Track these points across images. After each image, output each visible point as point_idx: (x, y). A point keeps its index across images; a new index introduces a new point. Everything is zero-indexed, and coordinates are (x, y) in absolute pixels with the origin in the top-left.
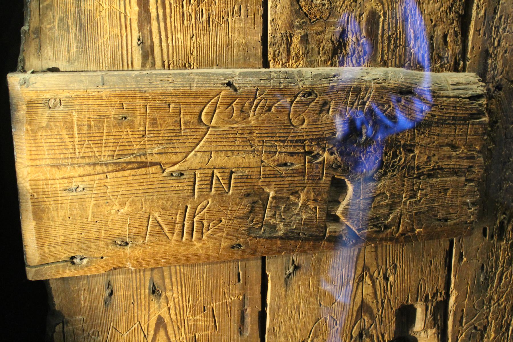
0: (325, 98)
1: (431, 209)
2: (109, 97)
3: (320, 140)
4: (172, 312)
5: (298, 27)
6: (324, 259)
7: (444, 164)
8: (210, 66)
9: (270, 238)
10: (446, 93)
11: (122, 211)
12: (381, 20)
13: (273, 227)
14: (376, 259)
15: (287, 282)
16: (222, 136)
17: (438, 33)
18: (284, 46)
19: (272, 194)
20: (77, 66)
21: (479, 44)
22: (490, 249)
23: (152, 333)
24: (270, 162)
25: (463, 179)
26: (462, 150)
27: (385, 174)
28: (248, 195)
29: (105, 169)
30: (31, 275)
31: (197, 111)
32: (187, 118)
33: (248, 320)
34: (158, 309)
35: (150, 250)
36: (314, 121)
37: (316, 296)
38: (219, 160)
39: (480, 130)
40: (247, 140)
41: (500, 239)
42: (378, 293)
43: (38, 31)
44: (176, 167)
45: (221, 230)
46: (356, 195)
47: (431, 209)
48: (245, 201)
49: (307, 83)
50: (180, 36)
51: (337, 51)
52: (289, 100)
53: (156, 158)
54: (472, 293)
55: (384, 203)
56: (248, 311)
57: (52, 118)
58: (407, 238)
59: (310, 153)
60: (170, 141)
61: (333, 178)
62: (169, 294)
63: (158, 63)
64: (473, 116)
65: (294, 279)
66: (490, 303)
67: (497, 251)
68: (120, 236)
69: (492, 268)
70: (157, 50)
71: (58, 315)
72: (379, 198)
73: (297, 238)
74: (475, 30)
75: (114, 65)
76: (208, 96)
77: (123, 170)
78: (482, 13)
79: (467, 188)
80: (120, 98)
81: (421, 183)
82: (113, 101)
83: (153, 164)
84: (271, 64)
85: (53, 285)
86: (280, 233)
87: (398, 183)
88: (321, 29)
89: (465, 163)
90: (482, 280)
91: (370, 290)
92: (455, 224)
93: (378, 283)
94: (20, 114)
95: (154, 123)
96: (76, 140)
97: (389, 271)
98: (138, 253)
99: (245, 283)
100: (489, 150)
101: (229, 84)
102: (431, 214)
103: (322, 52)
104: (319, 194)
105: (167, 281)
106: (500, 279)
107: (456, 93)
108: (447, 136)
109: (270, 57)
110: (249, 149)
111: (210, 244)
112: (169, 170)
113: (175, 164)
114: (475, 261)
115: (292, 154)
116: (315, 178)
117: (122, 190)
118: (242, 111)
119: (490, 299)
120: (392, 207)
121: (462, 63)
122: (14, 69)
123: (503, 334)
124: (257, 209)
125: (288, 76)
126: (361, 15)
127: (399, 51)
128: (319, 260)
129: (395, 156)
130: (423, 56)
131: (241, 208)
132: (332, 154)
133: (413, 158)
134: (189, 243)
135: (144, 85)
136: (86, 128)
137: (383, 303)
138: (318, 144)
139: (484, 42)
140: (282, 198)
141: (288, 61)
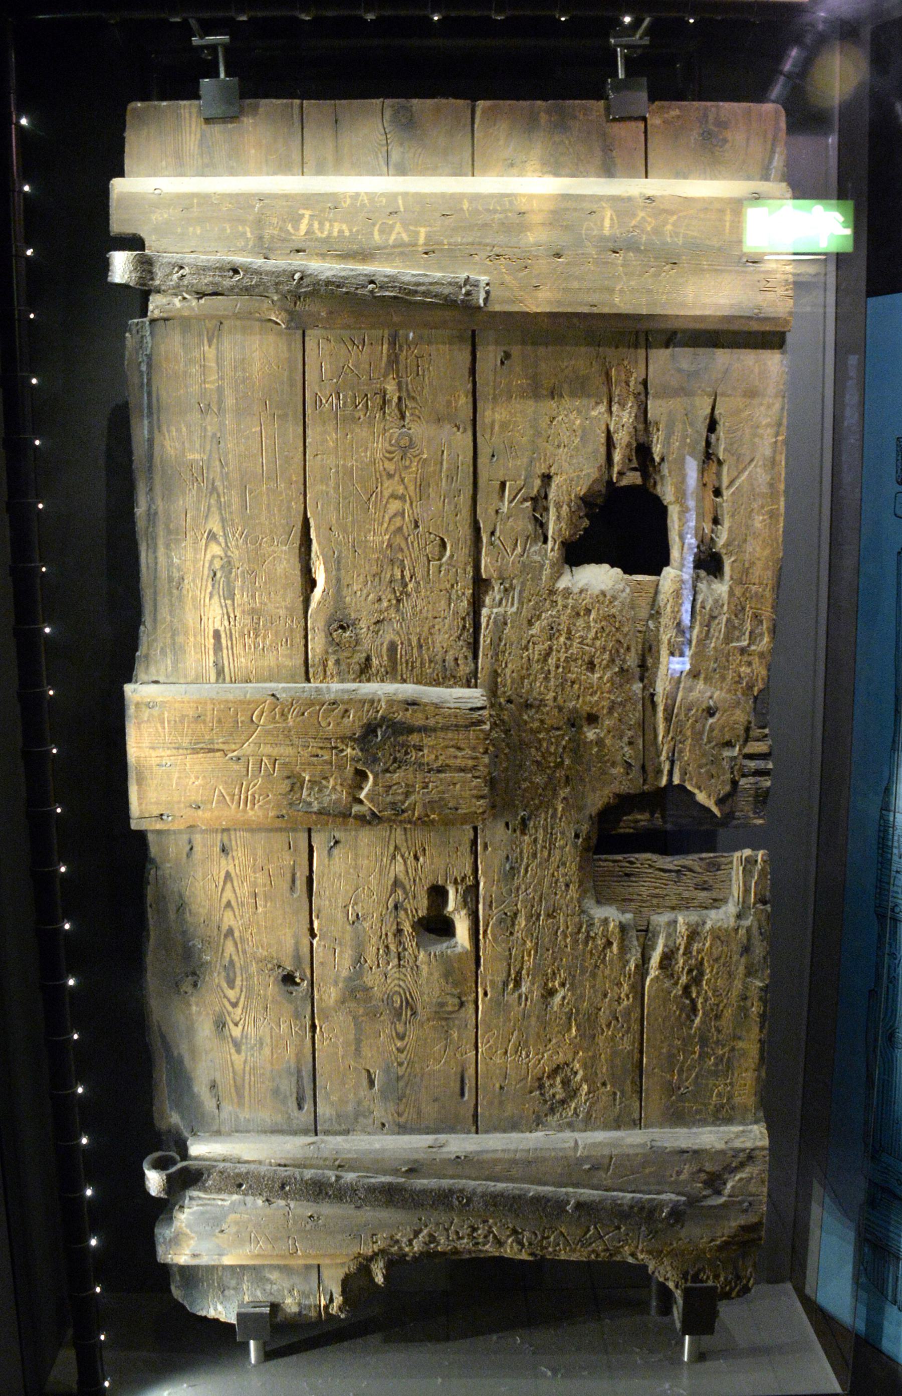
0: (346, 707)
1: (441, 799)
2: (189, 702)
3: (343, 739)
4: (237, 868)
5: (335, 652)
6: (360, 837)
7: (451, 762)
8: (265, 681)
9: (306, 812)
10: (448, 705)
11: (196, 783)
12: (399, 647)
13: (310, 804)
14: (406, 841)
15: (330, 854)
16: (268, 732)
17: (450, 657)
18: (321, 669)
19: (307, 778)
20: (171, 680)
21: (488, 666)
22: (513, 842)
23: (222, 883)
24: (305, 753)
25: (470, 775)
26: (468, 752)
27: (400, 767)
28: (289, 777)
29: (185, 752)
30: (134, 825)
31: (250, 713)
32: (243, 718)
33: (298, 883)
34: (226, 865)
35: (216, 813)
36: (338, 724)
37: (355, 868)
38: (266, 750)
39: (482, 736)
40: (288, 737)
41: (523, 833)
42: (410, 871)
43: (147, 656)
44: (235, 753)
45: (268, 802)
46: (375, 784)
47: (441, 799)
48: (286, 781)
49: (332, 696)
50: (243, 660)
51: (365, 671)
52: (318, 708)
53: (221, 746)
54: (499, 881)
55: (400, 791)
56: (298, 875)
57: (151, 715)
58: (424, 822)
59: (336, 748)
60: (231, 735)
61: (356, 769)
62: (235, 853)
63: (228, 679)
64: (474, 724)
65: (335, 852)
66: (518, 891)
67: (521, 843)
68: (195, 802)
69: (517, 859)
70: (226, 670)
71: (152, 861)
72: (395, 787)
73: (329, 814)
74: (484, 655)
75: (197, 679)
76: (258, 703)
77: (198, 753)
78: (488, 641)
79: (474, 784)
80: (196, 702)
81: (433, 776)
82: (192, 705)
83: (219, 750)
84: (312, 680)
85: (151, 838)
86: (315, 809)
87: (411, 776)
88: (350, 655)
89: (471, 763)
90: (508, 868)
91: (402, 868)
92: (465, 814)
93: (409, 862)
94: (131, 711)
95: (219, 721)
96: (167, 730)
97: (418, 854)
98: (208, 815)
99: (295, 850)
100: (505, 754)
101: (273, 695)
102: (443, 803)
103: (351, 672)
104: (345, 780)
105: (233, 843)
106: (526, 871)
107: (457, 705)
108: (451, 740)
109: (311, 675)
110: (288, 743)
111: (260, 813)
112: (230, 755)
113: (234, 751)
114: (500, 852)
115: (321, 748)
116: (341, 768)
117: (197, 768)
118: (283, 715)
119: (518, 889)
120: (407, 795)
121: (473, 681)
122: (129, 680)
123: (534, 923)
124: (296, 789)
125: (318, 690)
126: (382, 644)
127: (417, 671)
128: (356, 838)
129: (406, 753)
130: (437, 675)
131: (285, 786)
132: (354, 749)
133: (423, 756)
134: (245, 810)
135: (213, 695)
136: (173, 722)
137: (414, 881)
138: (342, 742)
139: (492, 664)
140: (315, 782)
141: (325, 678)
